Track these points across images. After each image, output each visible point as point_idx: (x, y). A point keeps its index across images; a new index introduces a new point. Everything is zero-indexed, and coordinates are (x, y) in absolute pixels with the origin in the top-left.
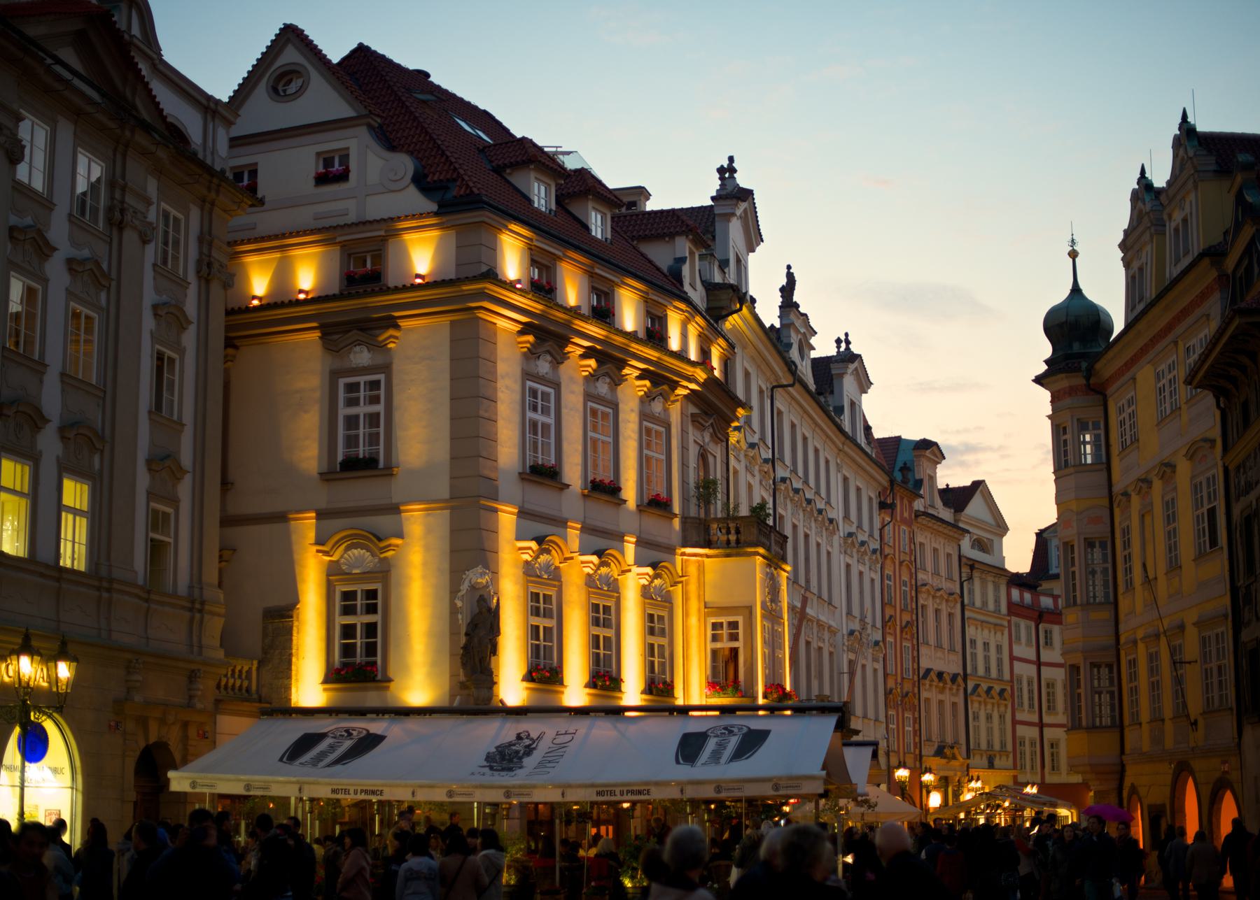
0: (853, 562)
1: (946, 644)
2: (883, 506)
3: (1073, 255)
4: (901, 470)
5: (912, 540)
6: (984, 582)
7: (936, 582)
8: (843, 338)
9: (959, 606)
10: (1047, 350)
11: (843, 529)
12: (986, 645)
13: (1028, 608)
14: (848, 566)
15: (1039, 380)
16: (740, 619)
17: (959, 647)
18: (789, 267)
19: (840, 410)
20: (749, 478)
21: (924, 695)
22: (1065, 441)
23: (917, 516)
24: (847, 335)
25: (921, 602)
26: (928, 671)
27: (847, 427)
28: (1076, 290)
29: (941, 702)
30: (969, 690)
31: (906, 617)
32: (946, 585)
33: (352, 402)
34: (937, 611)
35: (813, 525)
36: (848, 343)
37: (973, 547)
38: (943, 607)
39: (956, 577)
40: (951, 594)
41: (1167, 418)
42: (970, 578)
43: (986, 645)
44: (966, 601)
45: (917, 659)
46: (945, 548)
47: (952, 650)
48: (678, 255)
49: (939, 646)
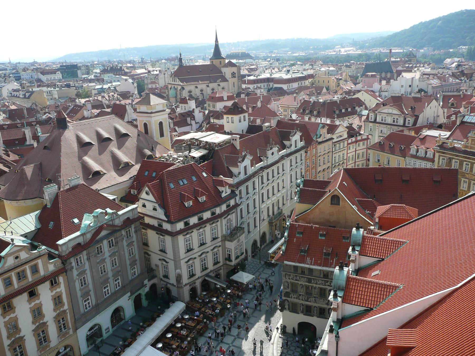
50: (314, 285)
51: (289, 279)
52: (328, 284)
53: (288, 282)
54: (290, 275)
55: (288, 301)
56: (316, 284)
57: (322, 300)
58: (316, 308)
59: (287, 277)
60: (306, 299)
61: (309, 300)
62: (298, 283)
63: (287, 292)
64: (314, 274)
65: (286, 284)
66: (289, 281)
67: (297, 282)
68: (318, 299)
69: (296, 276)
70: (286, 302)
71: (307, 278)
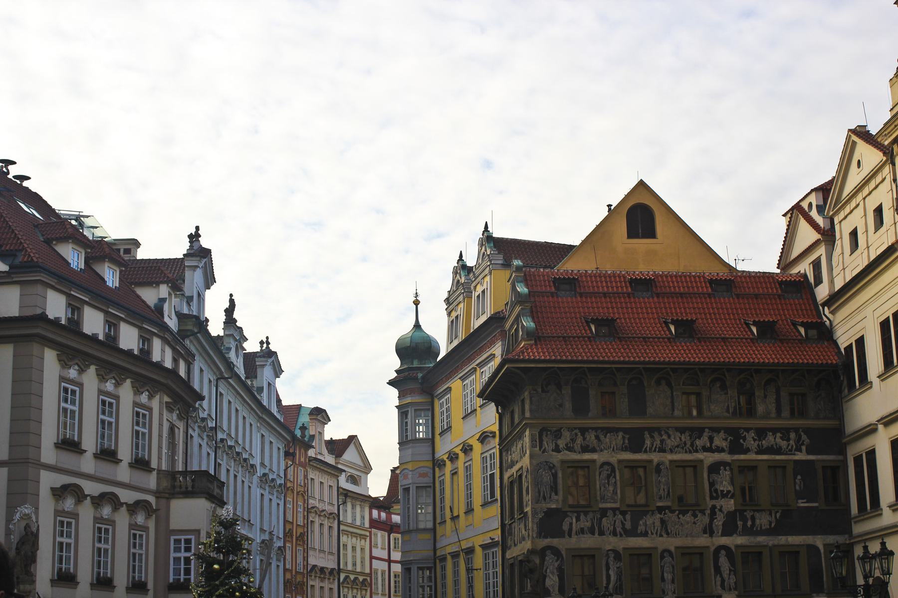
0: (266, 493)
2: (287, 454)
3: (416, 303)
4: (301, 428)
5: (306, 477)
6: (353, 507)
7: (321, 506)
8: (265, 340)
9: (336, 522)
11: (260, 471)
13: (384, 523)
14: (262, 495)
15: (391, 383)
17: (335, 551)
18: (231, 295)
19: (260, 390)
20: (200, 441)
21: (311, 583)
23: (310, 461)
24: (267, 338)
25: (311, 519)
26: (314, 566)
27: (265, 403)
28: (417, 326)
29: (322, 588)
30: (341, 580)
31: (300, 530)
32: (328, 508)
33: (178, 550)
34: (321, 525)
35: (240, 469)
36: (268, 343)
37: (347, 481)
38: (326, 522)
39: (335, 503)
40: (331, 514)
41: (469, 415)
42: (345, 503)
45: (306, 559)
46: (328, 481)
47: (331, 553)
48: (161, 297)
50: (656, 457)
51: (557, 450)
52: (703, 441)
53: (551, 467)
54: (558, 434)
55: (556, 552)
56: (662, 450)
57: (688, 517)
58: (668, 559)
59: (548, 444)
60: (628, 525)
61: (641, 528)
62: (594, 461)
63: (549, 513)
64: (650, 410)
65: (547, 477)
66: (556, 458)
67: (587, 456)
68: (674, 517)
69: (584, 431)
70: (549, 557)
71: (625, 431)
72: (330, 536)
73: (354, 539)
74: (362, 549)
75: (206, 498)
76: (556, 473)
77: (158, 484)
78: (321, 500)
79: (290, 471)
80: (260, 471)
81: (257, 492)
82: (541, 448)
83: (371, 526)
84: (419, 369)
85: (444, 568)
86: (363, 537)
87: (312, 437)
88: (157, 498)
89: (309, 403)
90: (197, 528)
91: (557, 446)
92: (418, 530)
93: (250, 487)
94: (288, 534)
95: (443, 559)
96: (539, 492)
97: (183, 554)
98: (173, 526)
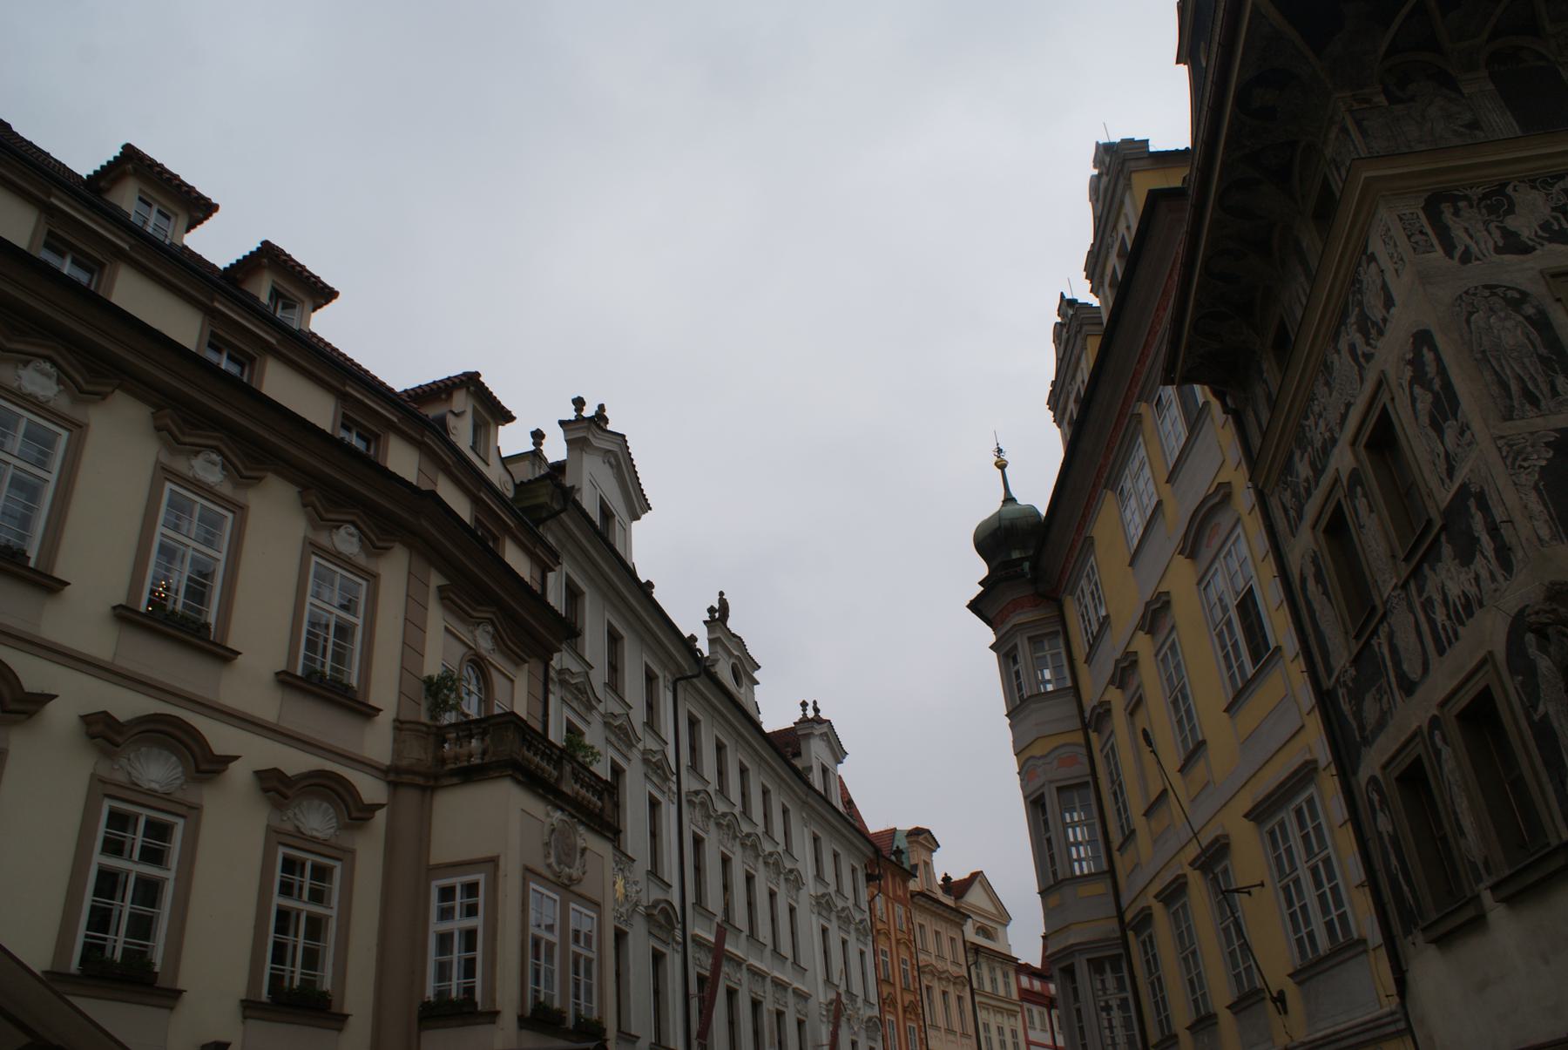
0: (833, 928)
1: (957, 1027)
2: (870, 878)
3: (1002, 466)
5: (909, 920)
6: (992, 970)
7: (940, 965)
9: (968, 988)
10: (980, 569)
12: (1000, 1030)
14: (824, 931)
16: (480, 877)
17: (971, 1031)
18: (721, 594)
19: (810, 769)
22: (1017, 673)
25: (925, 982)
28: (1009, 499)
31: (908, 998)
32: (953, 969)
34: (944, 993)
38: (951, 989)
39: (962, 960)
43: (1000, 1030)
44: (975, 985)
46: (947, 932)
47: (964, 1035)
49: (949, 1031)
53: (1517, 301)
54: (1497, 201)
65: (1512, 333)
72: (961, 1012)
73: (999, 1018)
74: (1014, 1033)
75: (519, 782)
76: (1542, 313)
77: (397, 753)
78: (940, 957)
79: (880, 902)
80: (811, 887)
81: (810, 923)
82: (1449, 249)
83: (1022, 999)
84: (1022, 560)
85: (1149, 944)
86: (1012, 1014)
87: (915, 867)
88: (394, 786)
89: (905, 825)
90: (489, 854)
91: (1508, 234)
92: (1074, 879)
93: (792, 910)
94: (886, 1002)
95: (1145, 918)
96: (1504, 386)
97: (459, 924)
98: (438, 855)
